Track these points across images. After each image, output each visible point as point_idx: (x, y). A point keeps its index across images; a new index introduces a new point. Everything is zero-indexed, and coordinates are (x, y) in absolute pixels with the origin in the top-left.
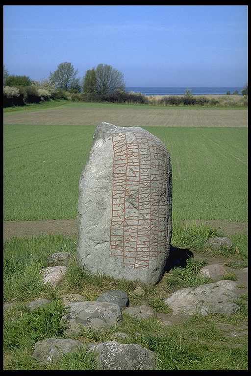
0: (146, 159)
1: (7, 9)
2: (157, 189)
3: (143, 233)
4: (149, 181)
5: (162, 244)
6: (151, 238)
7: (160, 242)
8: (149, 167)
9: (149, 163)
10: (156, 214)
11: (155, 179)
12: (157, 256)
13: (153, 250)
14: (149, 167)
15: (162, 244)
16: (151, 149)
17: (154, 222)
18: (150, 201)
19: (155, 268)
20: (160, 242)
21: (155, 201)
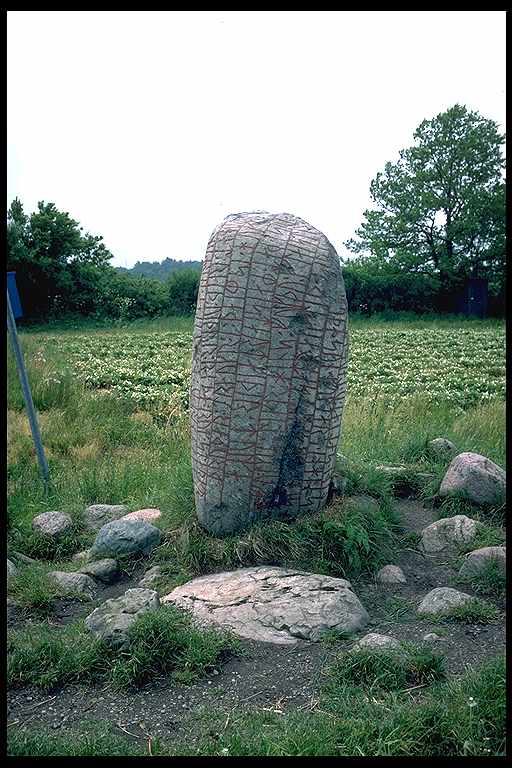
0: (217, 274)
1: (15, 19)
2: (236, 339)
3: (201, 425)
4: (216, 321)
5: (240, 458)
6: (213, 439)
7: (233, 452)
8: (221, 289)
9: (221, 281)
10: (226, 391)
11: (230, 317)
12: (222, 480)
13: (215, 465)
14: (221, 289)
15: (240, 458)
16: (236, 256)
17: (220, 406)
18: (215, 362)
19: (217, 502)
20: (233, 452)
21: (225, 364)
